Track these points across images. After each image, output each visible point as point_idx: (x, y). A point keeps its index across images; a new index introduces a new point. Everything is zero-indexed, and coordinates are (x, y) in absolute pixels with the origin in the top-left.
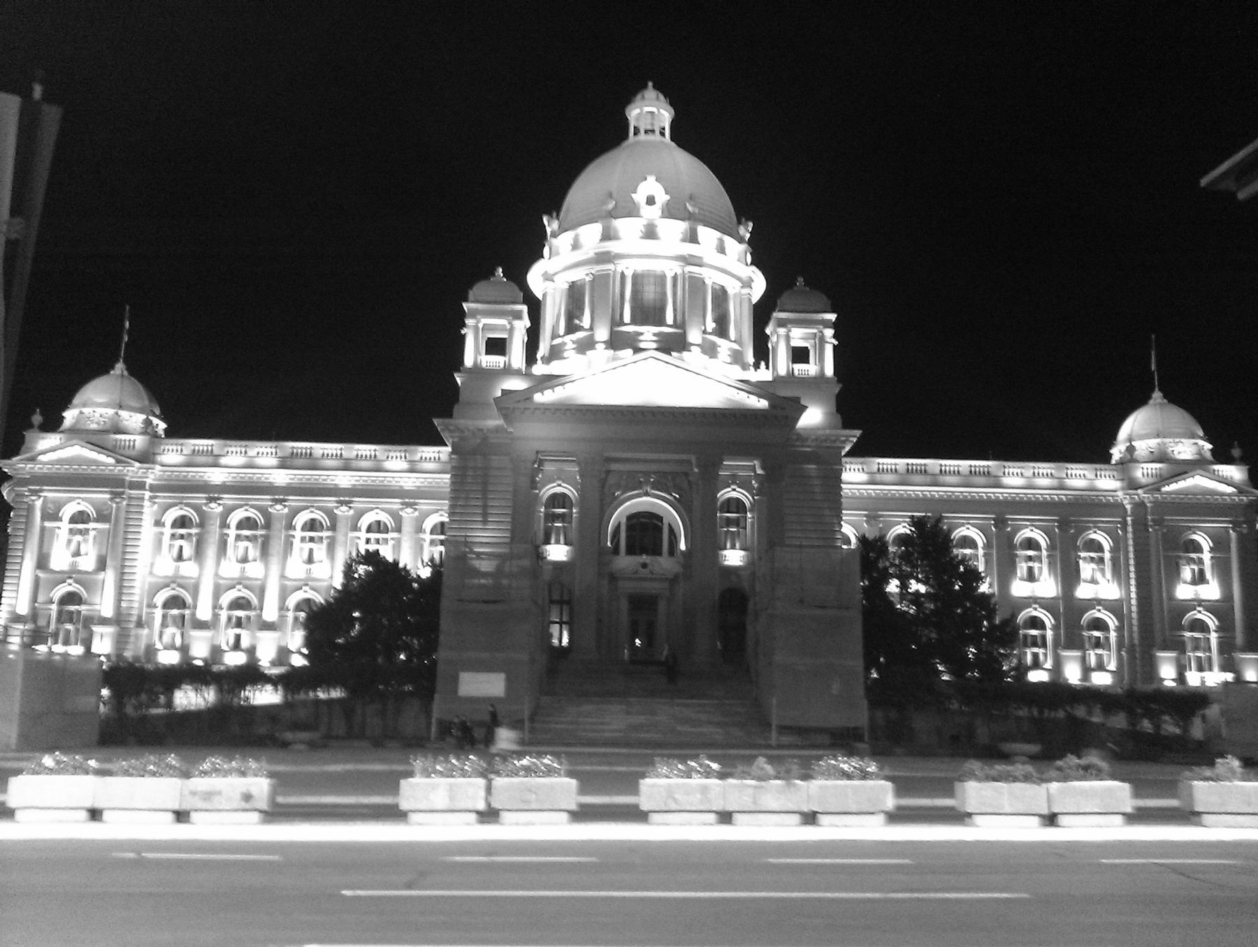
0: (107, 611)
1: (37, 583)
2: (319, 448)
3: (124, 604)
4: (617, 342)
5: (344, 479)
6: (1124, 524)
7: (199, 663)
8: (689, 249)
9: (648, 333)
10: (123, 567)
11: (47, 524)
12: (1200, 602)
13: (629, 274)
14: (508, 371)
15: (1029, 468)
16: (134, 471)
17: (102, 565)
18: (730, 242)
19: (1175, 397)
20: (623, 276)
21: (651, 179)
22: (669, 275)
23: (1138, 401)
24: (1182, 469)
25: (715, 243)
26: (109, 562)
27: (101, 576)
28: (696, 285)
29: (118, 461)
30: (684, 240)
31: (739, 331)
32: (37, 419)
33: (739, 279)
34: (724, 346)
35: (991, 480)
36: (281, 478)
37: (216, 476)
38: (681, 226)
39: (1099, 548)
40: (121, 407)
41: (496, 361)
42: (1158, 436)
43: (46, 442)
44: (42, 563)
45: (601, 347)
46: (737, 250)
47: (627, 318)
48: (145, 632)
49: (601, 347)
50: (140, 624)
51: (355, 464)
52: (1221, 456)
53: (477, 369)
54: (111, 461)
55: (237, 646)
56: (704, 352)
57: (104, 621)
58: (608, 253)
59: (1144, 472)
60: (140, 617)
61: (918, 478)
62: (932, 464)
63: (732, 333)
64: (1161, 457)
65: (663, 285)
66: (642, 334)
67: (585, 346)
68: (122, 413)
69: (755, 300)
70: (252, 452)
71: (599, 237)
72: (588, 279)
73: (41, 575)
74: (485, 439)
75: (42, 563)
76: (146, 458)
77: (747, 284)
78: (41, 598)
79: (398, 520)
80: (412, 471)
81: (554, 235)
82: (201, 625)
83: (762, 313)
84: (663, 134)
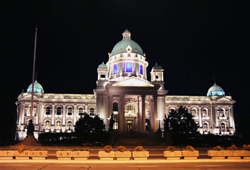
0: (37, 123)
1: (25, 118)
2: (70, 95)
3: (39, 122)
4: (124, 75)
5: (75, 101)
6: (210, 107)
7: (52, 132)
8: (136, 58)
9: (129, 74)
10: (39, 117)
11: (26, 108)
12: (206, 120)
13: (125, 63)
14: (106, 81)
15: (194, 97)
16: (40, 99)
17: (35, 115)
18: (143, 57)
19: (218, 85)
20: (124, 63)
21: (129, 46)
22: (133, 63)
23: (212, 85)
24: (220, 97)
25: (140, 57)
26: (37, 115)
27: (35, 117)
28: (137, 65)
29: (37, 97)
30: (135, 57)
31: (144, 73)
32: (23, 90)
33: (144, 64)
34: (142, 76)
35: (188, 99)
36: (64, 100)
37: (54, 100)
38: (134, 54)
39: (206, 111)
40: (37, 88)
41: (103, 79)
42: (216, 91)
43: (25, 94)
44: (25, 115)
45: (121, 76)
46: (144, 58)
47: (125, 71)
48: (43, 127)
49: (121, 76)
50: (42, 125)
51: (77, 98)
52: (227, 94)
53: (100, 80)
54: (36, 97)
55: (69, 130)
56: (139, 77)
57: (36, 125)
58: (122, 59)
59: (214, 97)
60: (42, 124)
61: (175, 99)
62: (178, 97)
63: (143, 74)
64: (217, 95)
65: (132, 65)
66: (128, 74)
67: (118, 76)
68: (37, 89)
69: (147, 67)
70: (59, 96)
71: (120, 56)
72: (118, 64)
73: (25, 117)
74: (102, 93)
75: (25, 115)
76: (42, 97)
77: (145, 65)
78: (25, 121)
79: (85, 107)
80: (87, 99)
81: (111, 56)
82: (52, 126)
83: (149, 70)
84: (129, 38)
